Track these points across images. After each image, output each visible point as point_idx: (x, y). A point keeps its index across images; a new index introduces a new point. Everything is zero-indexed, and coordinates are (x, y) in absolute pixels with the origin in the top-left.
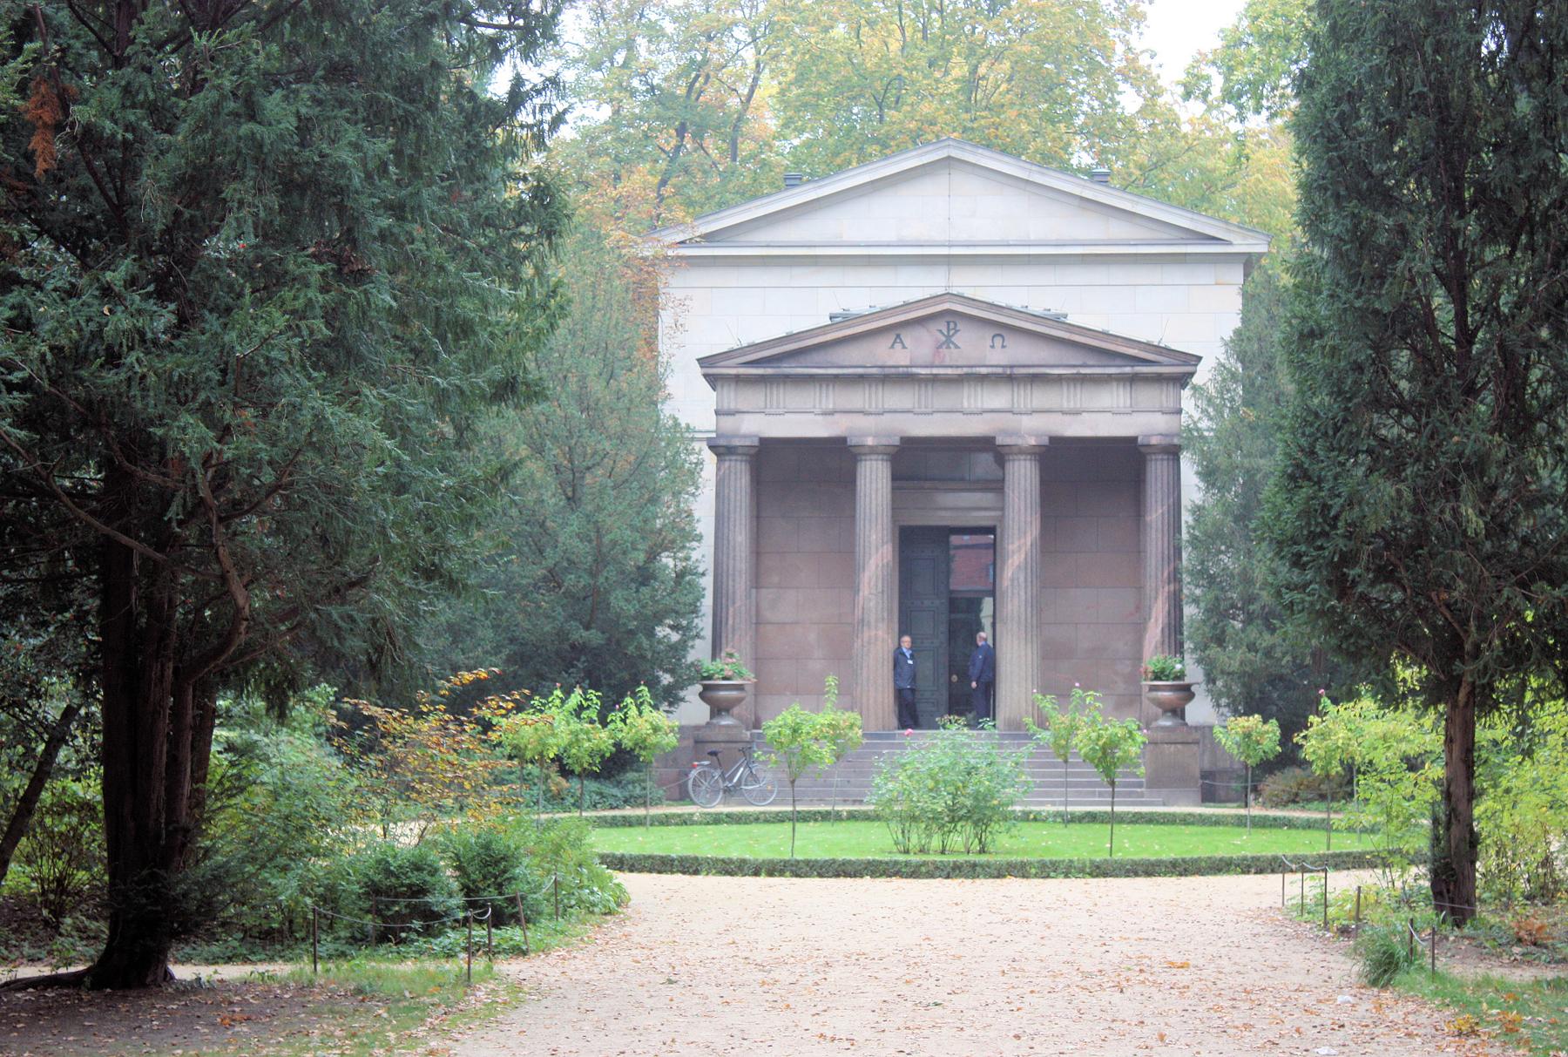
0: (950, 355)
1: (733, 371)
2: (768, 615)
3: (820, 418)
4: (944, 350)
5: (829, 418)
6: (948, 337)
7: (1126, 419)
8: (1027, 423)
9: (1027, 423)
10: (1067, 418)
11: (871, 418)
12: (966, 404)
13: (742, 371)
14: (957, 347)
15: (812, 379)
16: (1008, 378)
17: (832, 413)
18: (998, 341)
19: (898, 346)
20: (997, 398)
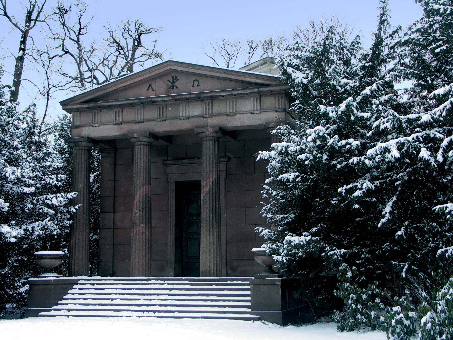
0: (175, 93)
1: (75, 107)
2: (119, 224)
3: (115, 126)
4: (171, 90)
5: (120, 126)
6: (173, 83)
7: (257, 116)
8: (210, 121)
9: (210, 121)
10: (229, 118)
11: (138, 124)
12: (181, 115)
13: (79, 106)
14: (177, 88)
15: (109, 107)
16: (199, 98)
17: (121, 124)
18: (196, 83)
19: (150, 90)
20: (196, 110)
